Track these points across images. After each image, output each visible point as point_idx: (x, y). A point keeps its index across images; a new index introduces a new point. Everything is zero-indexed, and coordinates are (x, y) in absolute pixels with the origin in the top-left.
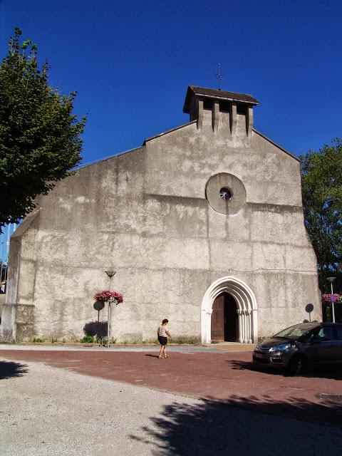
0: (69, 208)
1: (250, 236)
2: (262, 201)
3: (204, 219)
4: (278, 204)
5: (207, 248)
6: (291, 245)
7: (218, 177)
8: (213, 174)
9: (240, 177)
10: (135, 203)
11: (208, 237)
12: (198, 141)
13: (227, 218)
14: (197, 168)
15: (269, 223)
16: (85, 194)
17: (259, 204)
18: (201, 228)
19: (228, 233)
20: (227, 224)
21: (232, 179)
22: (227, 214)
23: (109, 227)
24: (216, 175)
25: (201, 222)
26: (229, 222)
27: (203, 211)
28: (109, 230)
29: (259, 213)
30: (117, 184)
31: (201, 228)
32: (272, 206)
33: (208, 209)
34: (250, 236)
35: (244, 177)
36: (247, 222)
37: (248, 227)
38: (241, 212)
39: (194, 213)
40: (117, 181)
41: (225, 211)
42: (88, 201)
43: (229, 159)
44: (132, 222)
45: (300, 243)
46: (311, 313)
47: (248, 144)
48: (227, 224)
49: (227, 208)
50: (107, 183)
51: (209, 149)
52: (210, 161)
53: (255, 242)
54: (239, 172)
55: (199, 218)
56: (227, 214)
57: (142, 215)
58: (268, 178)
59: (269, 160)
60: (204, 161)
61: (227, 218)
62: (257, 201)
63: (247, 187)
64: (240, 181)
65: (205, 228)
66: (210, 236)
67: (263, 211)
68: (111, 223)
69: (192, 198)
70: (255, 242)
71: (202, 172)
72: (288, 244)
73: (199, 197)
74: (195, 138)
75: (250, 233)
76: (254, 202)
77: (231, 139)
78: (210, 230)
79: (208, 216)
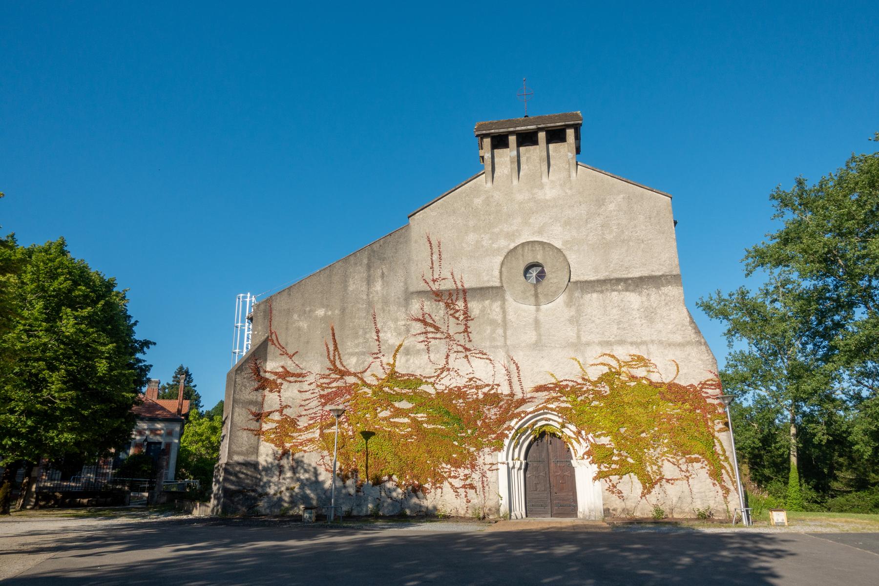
0: (305, 325)
1: (579, 337)
2: (601, 276)
3: (499, 318)
4: (630, 276)
5: (419, 332)
6: (661, 342)
7: (520, 251)
8: (512, 246)
9: (558, 244)
10: (393, 308)
11: (505, 345)
12: (487, 202)
13: (538, 310)
14: (486, 243)
15: (615, 311)
16: (327, 307)
17: (594, 281)
18: (493, 331)
19: (539, 335)
20: (537, 322)
21: (544, 249)
22: (537, 304)
23: (357, 345)
24: (516, 248)
25: (493, 322)
26: (541, 316)
27: (496, 306)
28: (357, 350)
29: (595, 295)
30: (368, 284)
31: (493, 331)
32: (619, 281)
33: (504, 300)
34: (579, 337)
35: (566, 243)
36: (573, 313)
37: (575, 321)
38: (561, 299)
39: (483, 311)
40: (369, 281)
41: (533, 299)
42: (330, 313)
43: (538, 220)
44: (389, 335)
45: (678, 338)
46: (152, 380)
47: (571, 189)
48: (537, 322)
49: (536, 296)
50: (356, 284)
51: (505, 209)
52: (506, 228)
53: (588, 344)
54: (556, 237)
55: (491, 317)
56: (537, 304)
57: (403, 323)
58: (609, 237)
59: (612, 207)
60: (496, 230)
61: (538, 310)
62: (592, 278)
63: (572, 258)
64: (559, 250)
65: (500, 331)
66: (508, 343)
67: (602, 292)
68: (361, 340)
69: (481, 289)
70: (588, 344)
71: (495, 246)
72: (652, 342)
73: (491, 284)
74: (482, 198)
75: (579, 331)
76: (586, 278)
77: (542, 186)
78: (509, 333)
79: (504, 312)
